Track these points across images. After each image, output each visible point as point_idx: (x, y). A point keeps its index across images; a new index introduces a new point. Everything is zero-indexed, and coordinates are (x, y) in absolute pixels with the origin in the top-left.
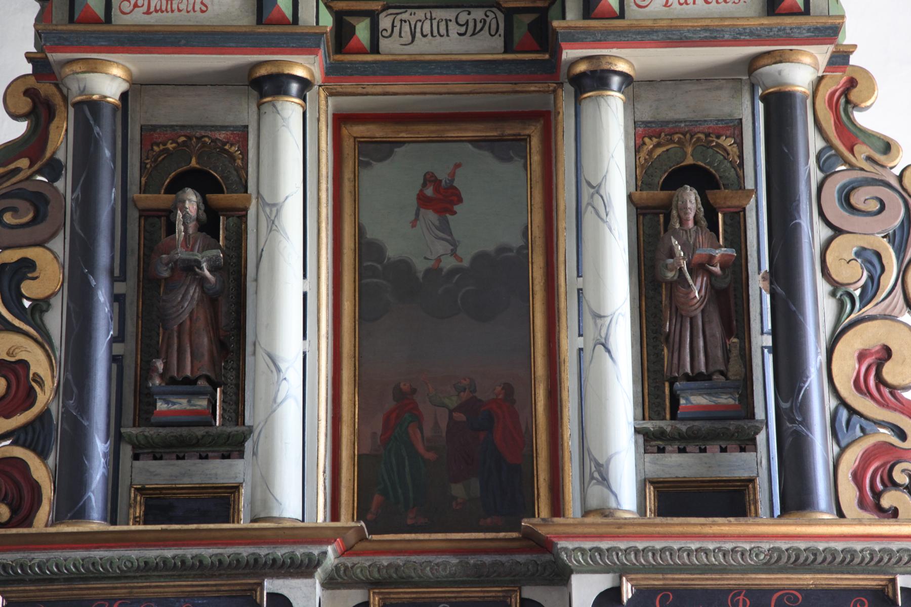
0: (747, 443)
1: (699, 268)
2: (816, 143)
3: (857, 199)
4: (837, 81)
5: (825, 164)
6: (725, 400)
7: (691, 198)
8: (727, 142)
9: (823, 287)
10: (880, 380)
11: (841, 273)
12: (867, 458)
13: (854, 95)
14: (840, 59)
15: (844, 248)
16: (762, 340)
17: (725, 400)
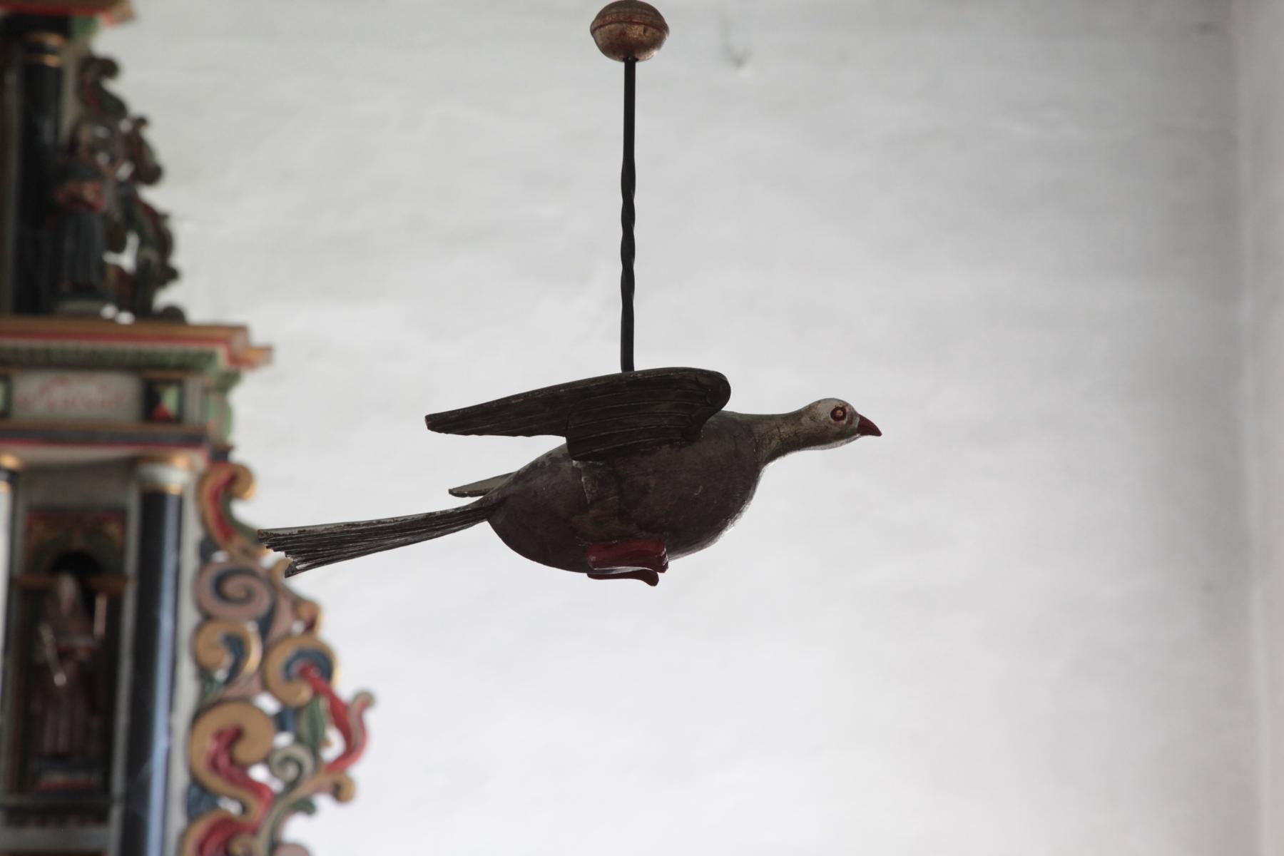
0: (101, 817)
1: (64, 655)
2: (193, 533)
3: (233, 587)
4: (222, 475)
5: (206, 550)
6: (81, 778)
7: (67, 588)
8: (113, 529)
9: (187, 671)
10: (232, 761)
11: (209, 657)
12: (213, 830)
13: (236, 489)
14: (221, 454)
15: (215, 633)
16: (122, 718)
17: (81, 778)
